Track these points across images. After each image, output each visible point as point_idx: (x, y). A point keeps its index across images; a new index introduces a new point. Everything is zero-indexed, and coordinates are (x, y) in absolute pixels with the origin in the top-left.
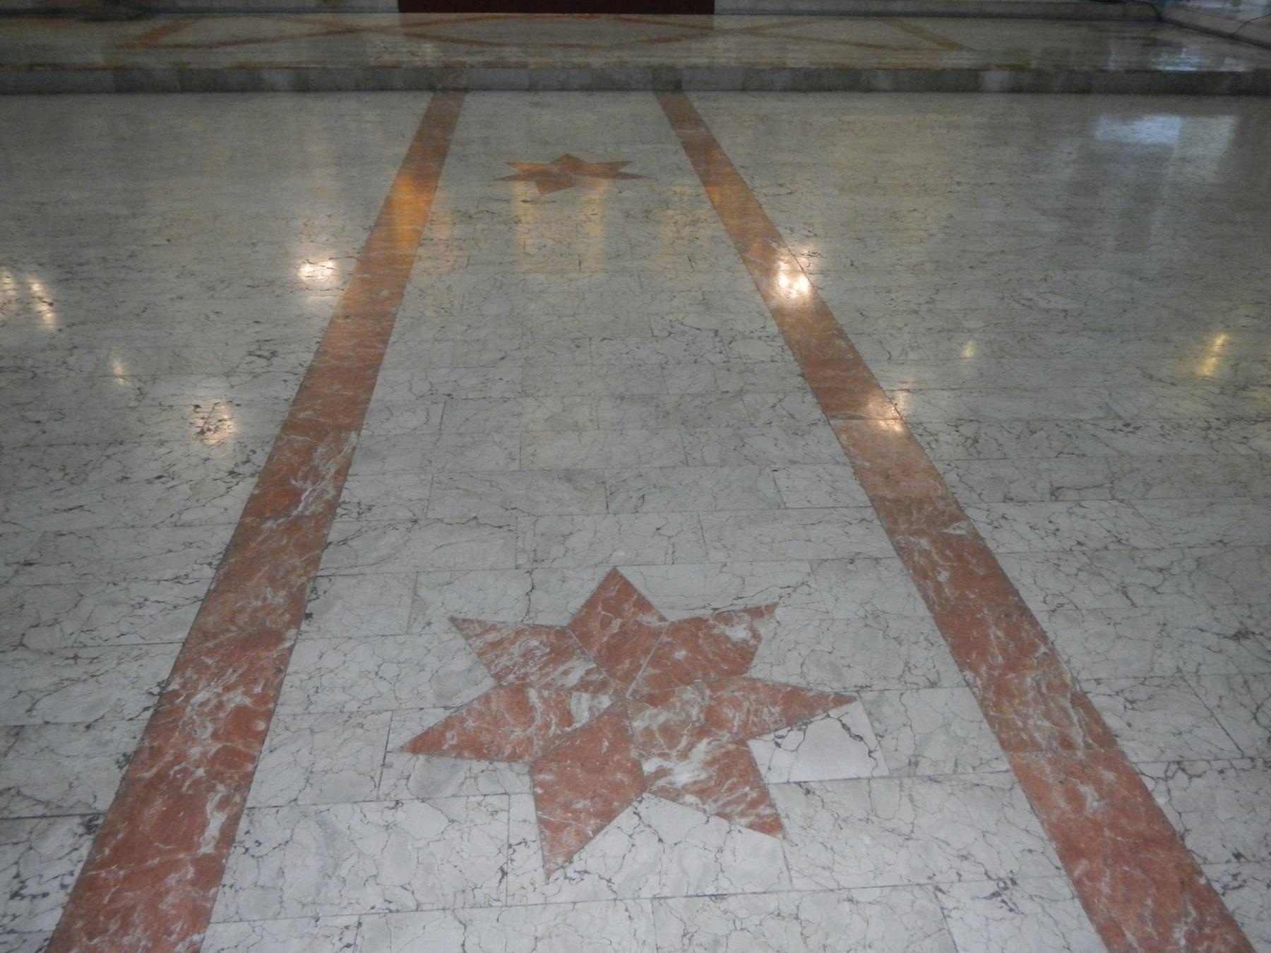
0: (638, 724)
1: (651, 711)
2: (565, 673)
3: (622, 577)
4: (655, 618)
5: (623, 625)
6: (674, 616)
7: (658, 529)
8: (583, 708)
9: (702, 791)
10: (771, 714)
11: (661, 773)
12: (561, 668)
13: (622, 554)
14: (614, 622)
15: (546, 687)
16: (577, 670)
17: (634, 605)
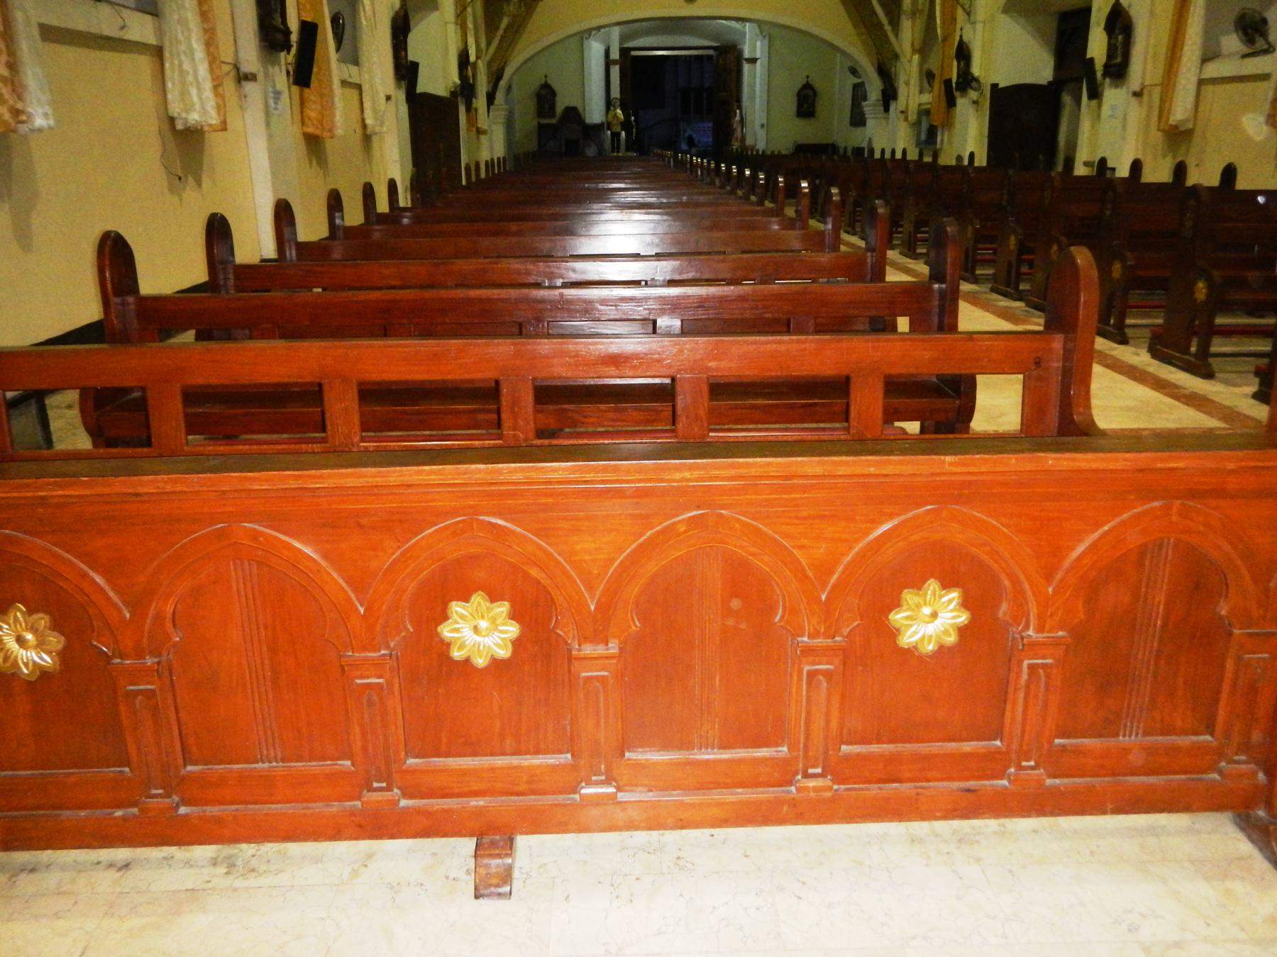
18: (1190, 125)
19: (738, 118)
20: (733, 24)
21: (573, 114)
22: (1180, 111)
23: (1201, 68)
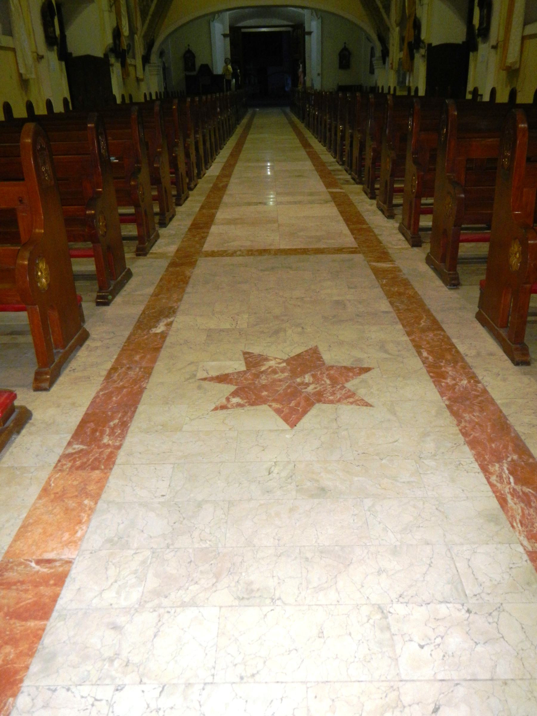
0: (286, 374)
1: (280, 378)
2: (315, 388)
3: (288, 424)
4: (273, 406)
5: (290, 404)
6: (265, 407)
7: (264, 450)
8: (308, 378)
9: (267, 359)
10: (234, 376)
11: (279, 363)
12: (317, 389)
13: (287, 436)
14: (294, 405)
15: (323, 384)
16: (310, 389)
17: (283, 411)
18: (517, 66)
19: (301, 70)
20: (300, 10)
21: (206, 69)
22: (512, 57)
23: (524, 29)
